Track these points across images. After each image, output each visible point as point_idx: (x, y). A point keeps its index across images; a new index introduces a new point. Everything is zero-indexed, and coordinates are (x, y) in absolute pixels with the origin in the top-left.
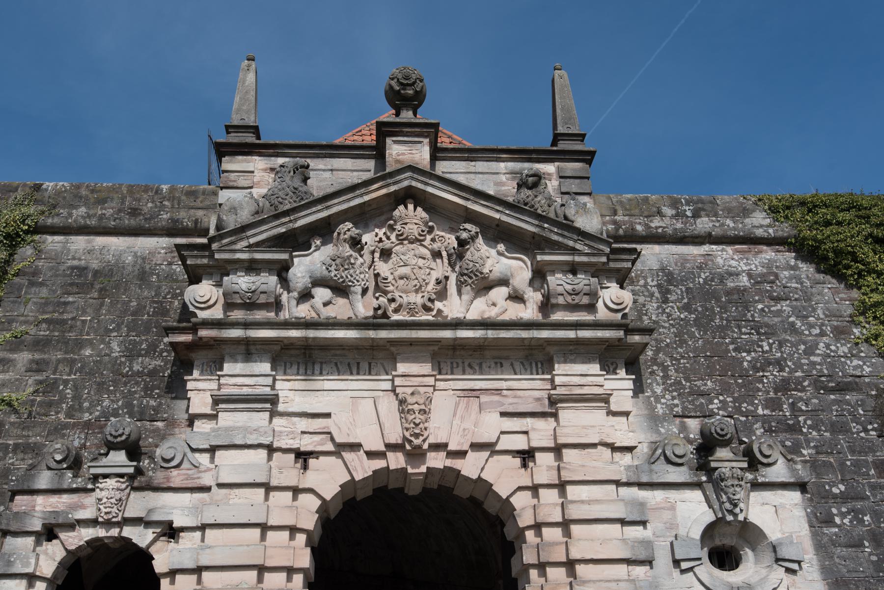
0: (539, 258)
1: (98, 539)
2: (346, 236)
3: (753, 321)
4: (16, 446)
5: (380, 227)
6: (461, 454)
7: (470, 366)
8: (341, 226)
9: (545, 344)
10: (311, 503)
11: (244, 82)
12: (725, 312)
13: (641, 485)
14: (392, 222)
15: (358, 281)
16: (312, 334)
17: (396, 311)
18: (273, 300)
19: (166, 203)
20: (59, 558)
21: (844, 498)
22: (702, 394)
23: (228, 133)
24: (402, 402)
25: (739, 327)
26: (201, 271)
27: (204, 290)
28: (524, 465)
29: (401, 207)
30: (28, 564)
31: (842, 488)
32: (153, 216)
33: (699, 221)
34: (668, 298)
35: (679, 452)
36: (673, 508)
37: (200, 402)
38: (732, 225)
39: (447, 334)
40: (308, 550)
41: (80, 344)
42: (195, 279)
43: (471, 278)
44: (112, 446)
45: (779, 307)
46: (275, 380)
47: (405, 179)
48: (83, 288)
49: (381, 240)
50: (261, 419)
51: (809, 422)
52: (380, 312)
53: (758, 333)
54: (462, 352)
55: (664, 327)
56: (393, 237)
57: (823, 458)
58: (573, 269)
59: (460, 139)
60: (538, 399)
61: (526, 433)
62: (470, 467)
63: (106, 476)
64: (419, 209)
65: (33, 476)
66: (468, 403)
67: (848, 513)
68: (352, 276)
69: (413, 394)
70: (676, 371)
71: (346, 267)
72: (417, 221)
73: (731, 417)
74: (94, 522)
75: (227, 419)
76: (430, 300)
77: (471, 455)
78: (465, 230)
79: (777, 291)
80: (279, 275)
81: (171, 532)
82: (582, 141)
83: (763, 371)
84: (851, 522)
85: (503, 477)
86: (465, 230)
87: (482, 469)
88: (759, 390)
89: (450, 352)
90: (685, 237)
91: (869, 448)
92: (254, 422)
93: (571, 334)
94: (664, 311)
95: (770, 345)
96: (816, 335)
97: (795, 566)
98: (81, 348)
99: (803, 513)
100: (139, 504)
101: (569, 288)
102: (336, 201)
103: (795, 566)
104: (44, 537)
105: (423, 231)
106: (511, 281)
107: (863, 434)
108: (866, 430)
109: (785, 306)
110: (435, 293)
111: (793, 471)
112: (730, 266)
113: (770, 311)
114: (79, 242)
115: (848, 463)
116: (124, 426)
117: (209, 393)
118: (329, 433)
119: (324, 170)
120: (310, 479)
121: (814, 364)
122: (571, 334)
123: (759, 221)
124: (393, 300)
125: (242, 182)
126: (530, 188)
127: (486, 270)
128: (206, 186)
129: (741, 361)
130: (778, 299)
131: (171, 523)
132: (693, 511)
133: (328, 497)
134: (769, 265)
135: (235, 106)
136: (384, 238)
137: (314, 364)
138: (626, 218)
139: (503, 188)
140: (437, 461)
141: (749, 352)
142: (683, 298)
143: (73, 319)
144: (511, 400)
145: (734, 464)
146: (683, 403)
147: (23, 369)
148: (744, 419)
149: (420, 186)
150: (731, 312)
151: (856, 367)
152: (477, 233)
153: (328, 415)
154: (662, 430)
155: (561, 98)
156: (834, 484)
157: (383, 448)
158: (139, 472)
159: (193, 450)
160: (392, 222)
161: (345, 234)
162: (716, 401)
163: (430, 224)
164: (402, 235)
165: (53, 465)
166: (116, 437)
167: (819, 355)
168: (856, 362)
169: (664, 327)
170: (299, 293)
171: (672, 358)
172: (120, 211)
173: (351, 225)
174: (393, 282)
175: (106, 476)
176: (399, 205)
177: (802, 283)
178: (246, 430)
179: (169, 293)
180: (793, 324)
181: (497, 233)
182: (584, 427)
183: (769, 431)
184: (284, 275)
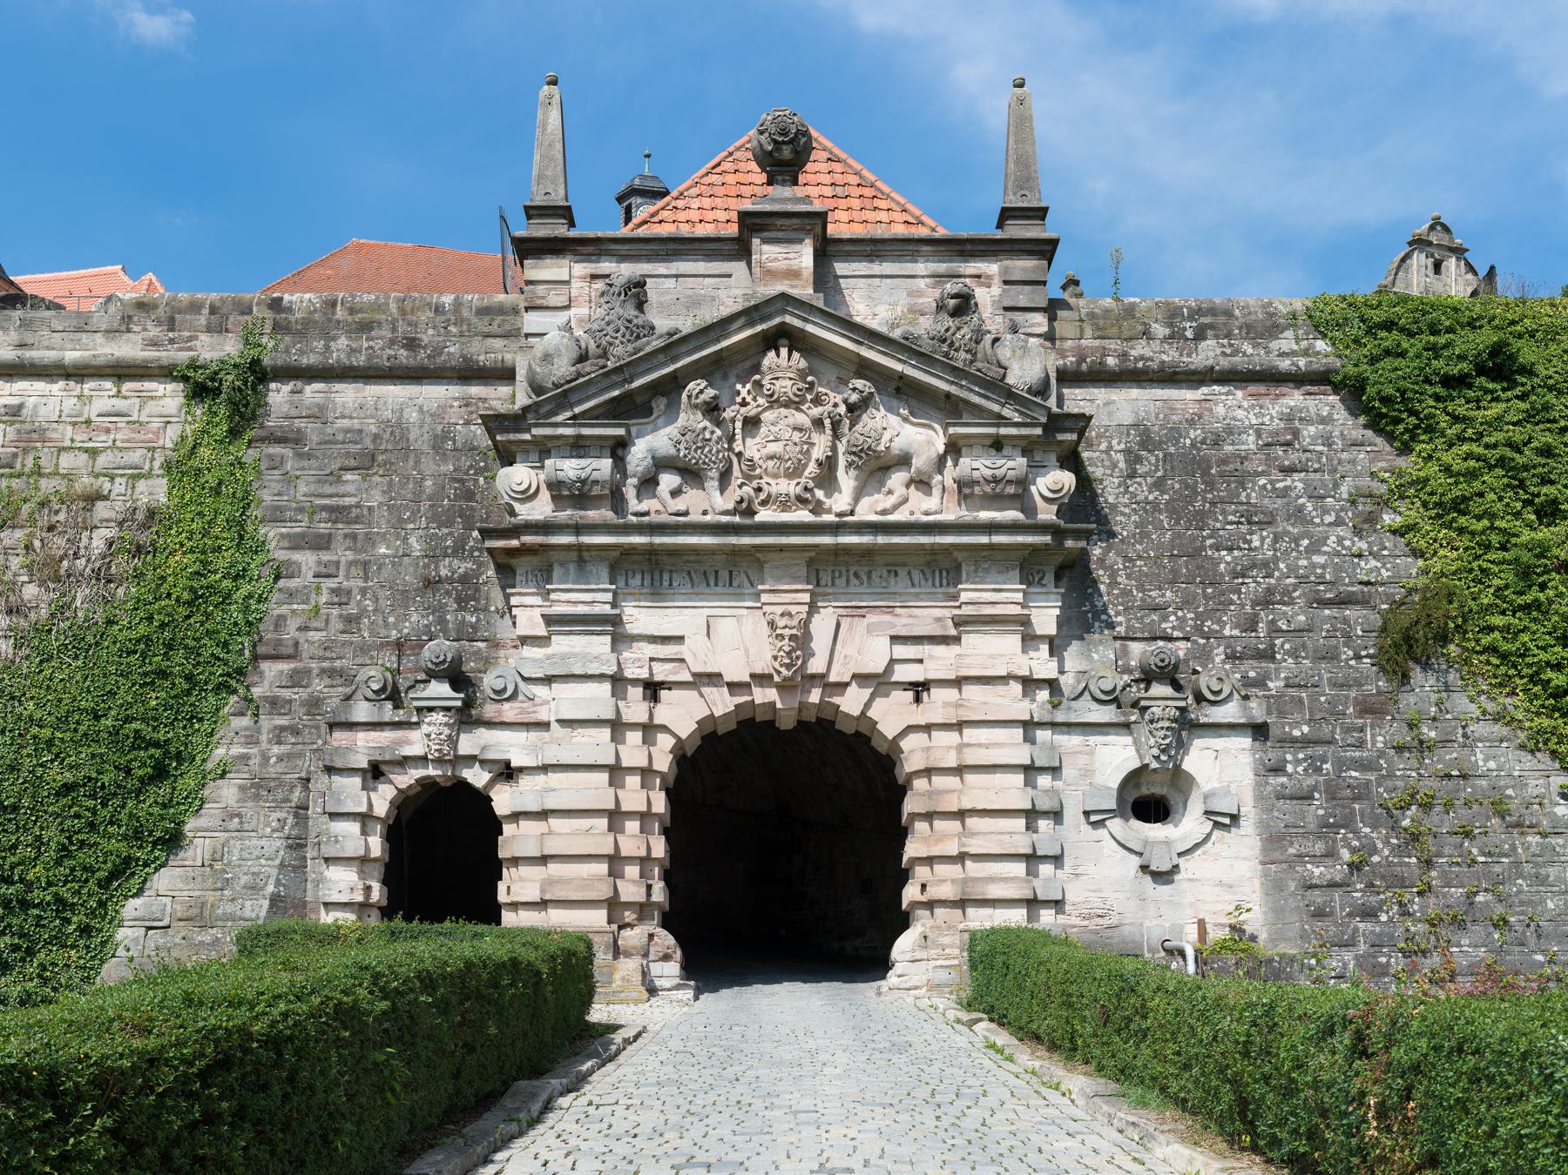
0: (951, 430)
1: (428, 777)
3: (1248, 503)
4: (323, 671)
6: (842, 686)
7: (856, 575)
8: (691, 385)
10: (665, 742)
11: (545, 125)
12: (1211, 491)
13: (1053, 725)
14: (757, 377)
17: (764, 503)
19: (453, 329)
20: (389, 798)
21: (1306, 742)
22: (1155, 609)
23: (529, 217)
24: (772, 624)
25: (1224, 512)
26: (513, 448)
27: (519, 475)
28: (918, 700)
29: (772, 354)
30: (360, 804)
31: (1306, 729)
32: (438, 351)
33: (1203, 344)
34: (1135, 471)
35: (1108, 687)
36: (1092, 753)
37: (529, 619)
38: (1250, 351)
40: (663, 794)
41: (370, 539)
42: (508, 459)
44: (432, 675)
45: (1288, 483)
46: (615, 594)
48: (366, 463)
50: (600, 645)
51: (1287, 646)
52: (744, 505)
53: (1249, 523)
54: (847, 558)
55: (1123, 514)
57: (1293, 692)
58: (997, 445)
59: (872, 178)
60: (939, 620)
61: (921, 661)
62: (851, 702)
63: (431, 709)
64: (796, 355)
65: (348, 709)
66: (851, 624)
67: (1305, 760)
69: (782, 615)
70: (1128, 577)
73: (1187, 639)
74: (423, 760)
75: (563, 644)
76: (806, 489)
77: (853, 689)
78: (854, 389)
79: (1293, 457)
80: (613, 455)
81: (507, 773)
82: (1043, 219)
83: (1244, 576)
84: (1305, 770)
85: (890, 715)
86: (854, 389)
87: (868, 705)
88: (1232, 603)
89: (832, 558)
90: (1175, 373)
91: (1355, 679)
92: (594, 649)
93: (984, 540)
94: (1126, 491)
95: (1263, 539)
96: (1330, 524)
97: (1227, 821)
98: (374, 546)
99: (1250, 759)
100: (468, 743)
101: (988, 473)
102: (684, 349)
103: (1227, 821)
104: (369, 775)
107: (1352, 662)
108: (1358, 657)
109: (1297, 482)
110: (813, 479)
111: (1245, 708)
112: (1234, 419)
113: (1274, 489)
114: (347, 394)
115: (1323, 699)
116: (439, 649)
117: (537, 612)
118: (682, 660)
119: (666, 276)
120: (662, 715)
121: (1314, 566)
122: (984, 540)
123: (1286, 352)
124: (759, 490)
125: (556, 298)
126: (952, 315)
127: (881, 448)
128: (501, 297)
129: (1216, 563)
130: (1288, 471)
131: (507, 764)
132: (1115, 758)
133: (684, 736)
134: (1288, 418)
135: (535, 172)
136: (749, 399)
137: (661, 573)
138: (1097, 343)
139: (921, 301)
140: (815, 696)
141: (1230, 549)
142: (1157, 470)
143: (358, 506)
144: (904, 621)
145: (1170, 703)
146: (1129, 620)
147: (311, 574)
148: (1202, 641)
150: (1219, 490)
151: (1371, 570)
152: (871, 394)
153: (679, 639)
154: (1096, 656)
155: (1017, 142)
156: (1297, 724)
157: (748, 679)
158: (468, 704)
159: (525, 679)
162: (1172, 618)
163: (810, 378)
165: (370, 695)
166: (436, 664)
167: (1325, 553)
168: (1373, 563)
169: (1123, 514)
171: (1126, 558)
172: (392, 342)
175: (431, 709)
176: (769, 349)
177: (1330, 445)
178: (585, 657)
179: (471, 467)
180: (1301, 509)
181: (903, 392)
182: (991, 656)
183: (1231, 657)
184: (620, 452)
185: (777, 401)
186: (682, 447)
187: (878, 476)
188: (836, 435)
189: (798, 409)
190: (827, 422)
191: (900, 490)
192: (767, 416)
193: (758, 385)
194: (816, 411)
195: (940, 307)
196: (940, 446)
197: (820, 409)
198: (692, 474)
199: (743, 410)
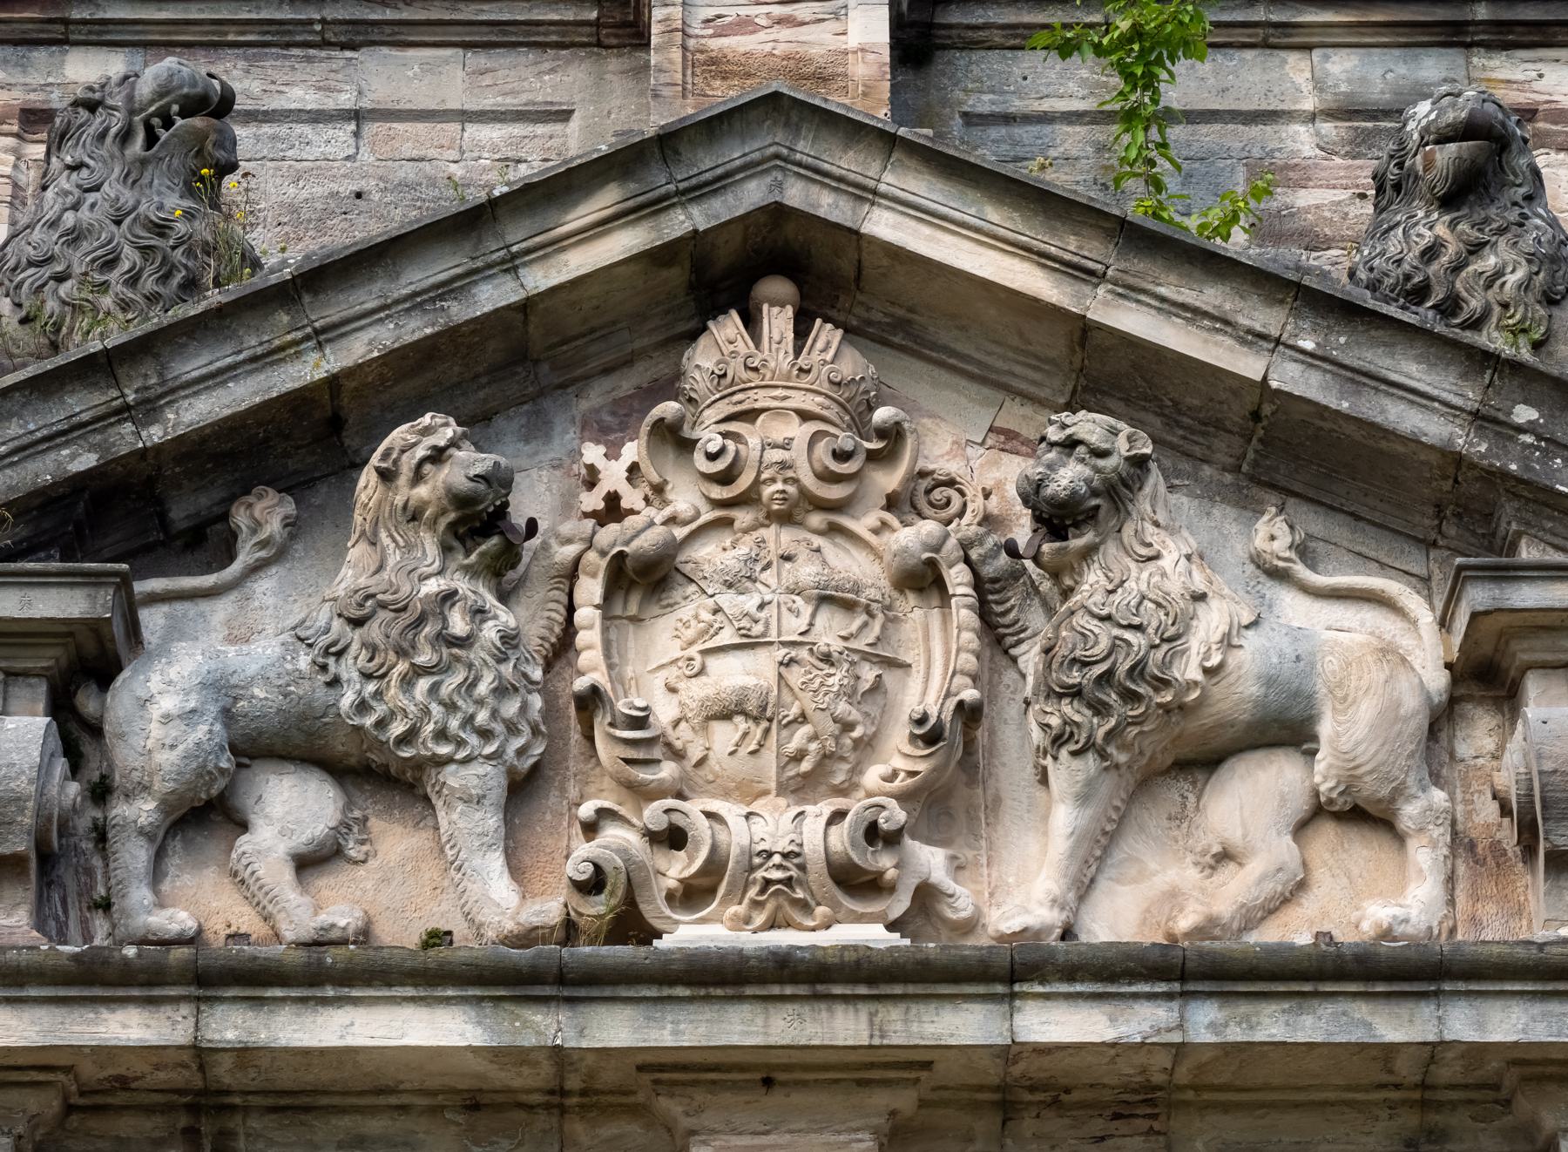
0: (1478, 596)
2: (423, 491)
5: (610, 434)
9: (1511, 1078)
14: (668, 409)
15: (485, 734)
16: (231, 1026)
17: (692, 895)
18: (20, 844)
29: (729, 328)
39: (963, 1025)
43: (1100, 709)
47: (751, 168)
49: (613, 510)
56: (686, 498)
64: (826, 335)
68: (451, 707)
71: (425, 657)
72: (811, 403)
76: (872, 833)
78: (1070, 444)
80: (61, 708)
105: (842, 456)
106: (1325, 729)
110: (903, 797)
124: (673, 838)
127: (1189, 670)
136: (631, 498)
149: (828, 205)
152: (1139, 463)
160: (668, 409)
161: (418, 477)
163: (882, 414)
164: (726, 478)
170: (165, 805)
173: (448, 431)
174: (682, 736)
176: (718, 311)
185: (747, 499)
186: (348, 669)
187: (1174, 792)
188: (997, 636)
189: (834, 530)
190: (958, 578)
191: (1272, 851)
192: (713, 555)
193: (674, 439)
194: (911, 537)
195: (1391, 188)
196: (1427, 657)
197: (928, 528)
198: (382, 777)
199: (609, 534)
